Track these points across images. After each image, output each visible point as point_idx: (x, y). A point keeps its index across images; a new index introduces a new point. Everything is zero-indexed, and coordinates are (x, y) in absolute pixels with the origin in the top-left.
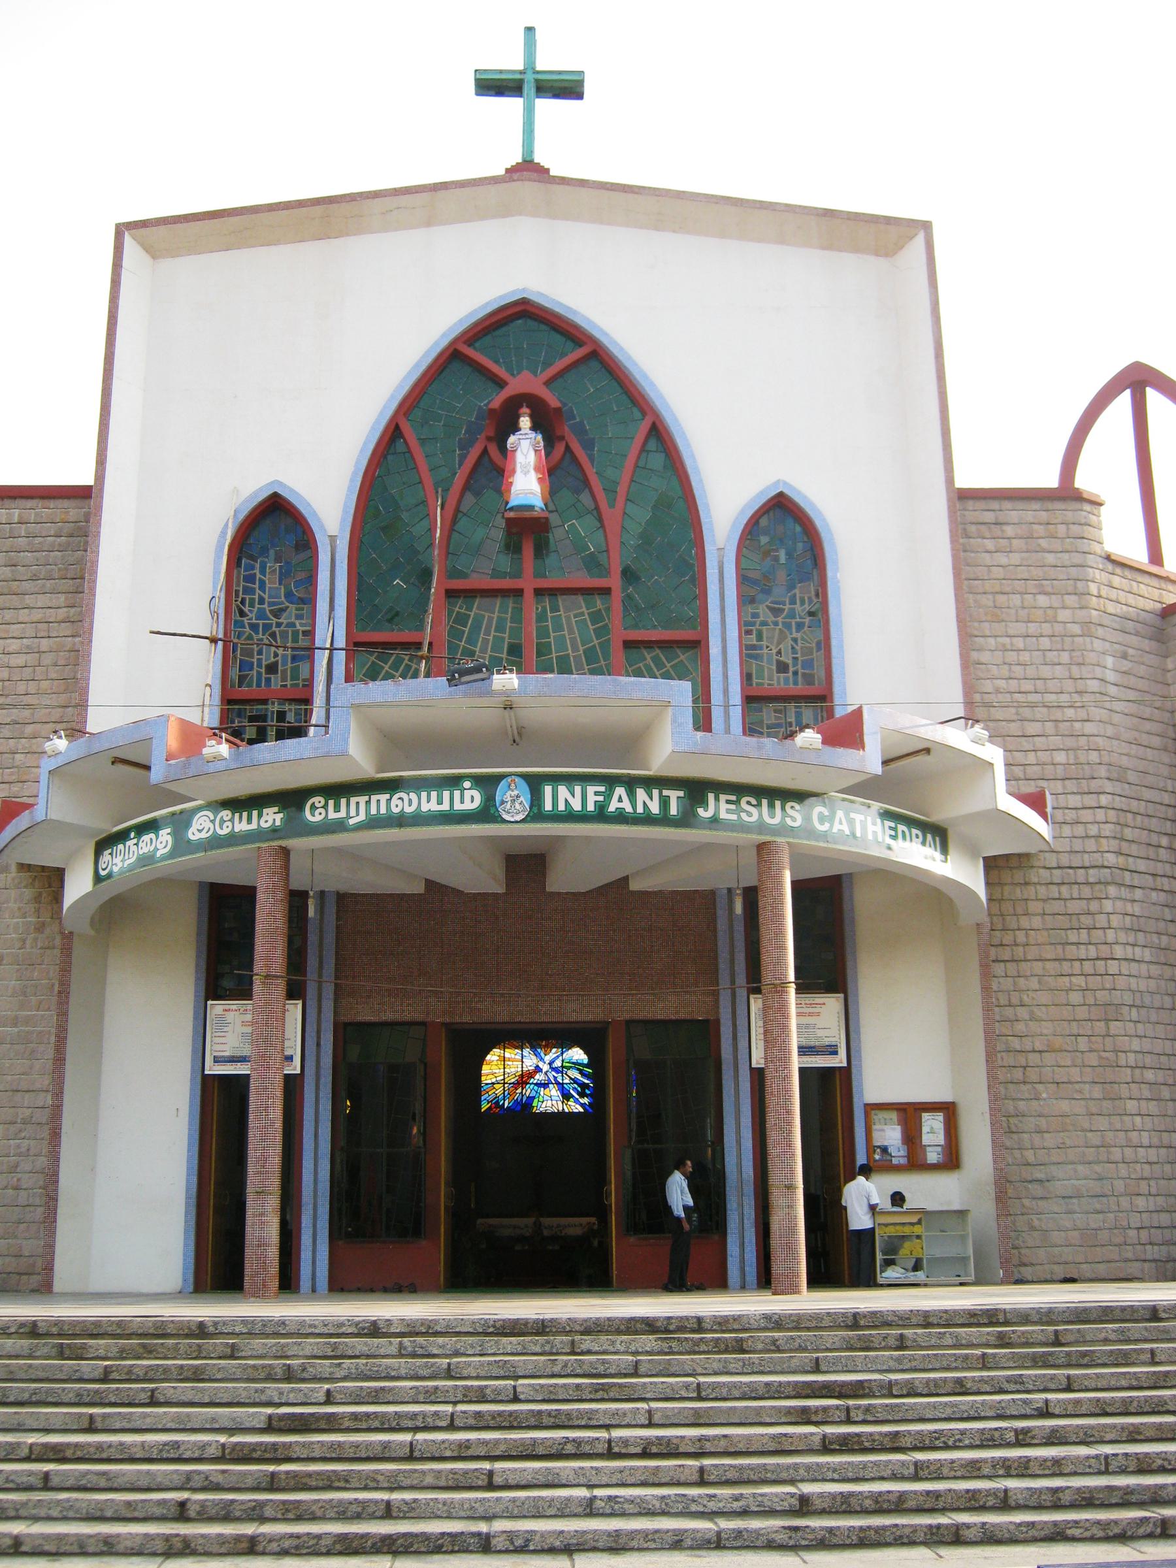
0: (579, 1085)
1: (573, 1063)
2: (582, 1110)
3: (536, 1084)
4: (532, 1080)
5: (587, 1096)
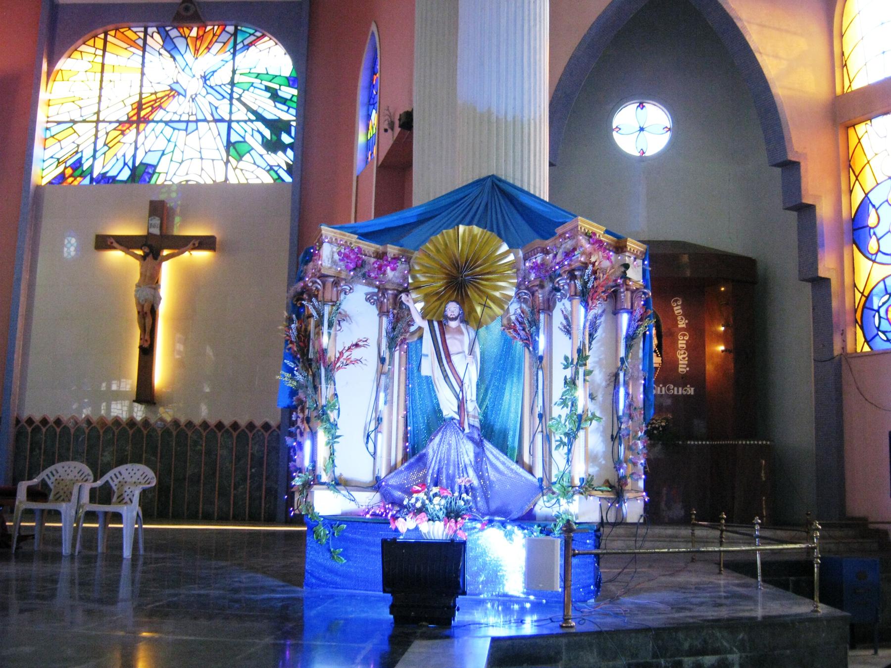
0: (268, 123)
1: (258, 76)
2: (267, 179)
3: (167, 123)
4: (159, 115)
5: (283, 147)
